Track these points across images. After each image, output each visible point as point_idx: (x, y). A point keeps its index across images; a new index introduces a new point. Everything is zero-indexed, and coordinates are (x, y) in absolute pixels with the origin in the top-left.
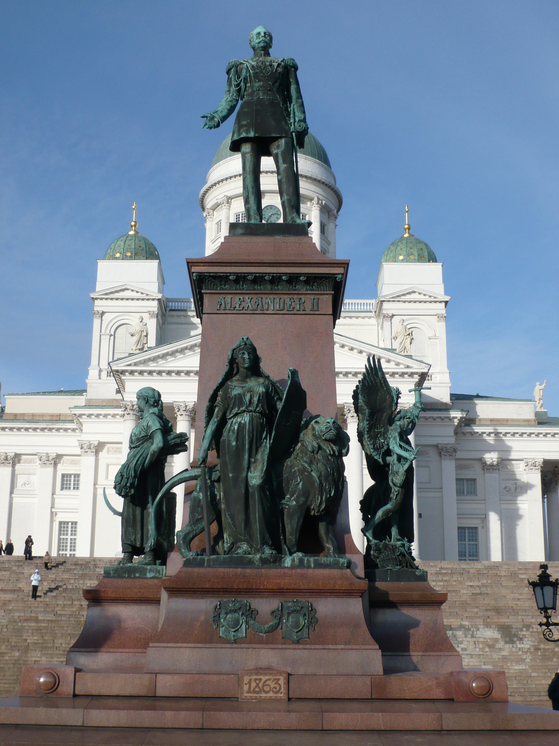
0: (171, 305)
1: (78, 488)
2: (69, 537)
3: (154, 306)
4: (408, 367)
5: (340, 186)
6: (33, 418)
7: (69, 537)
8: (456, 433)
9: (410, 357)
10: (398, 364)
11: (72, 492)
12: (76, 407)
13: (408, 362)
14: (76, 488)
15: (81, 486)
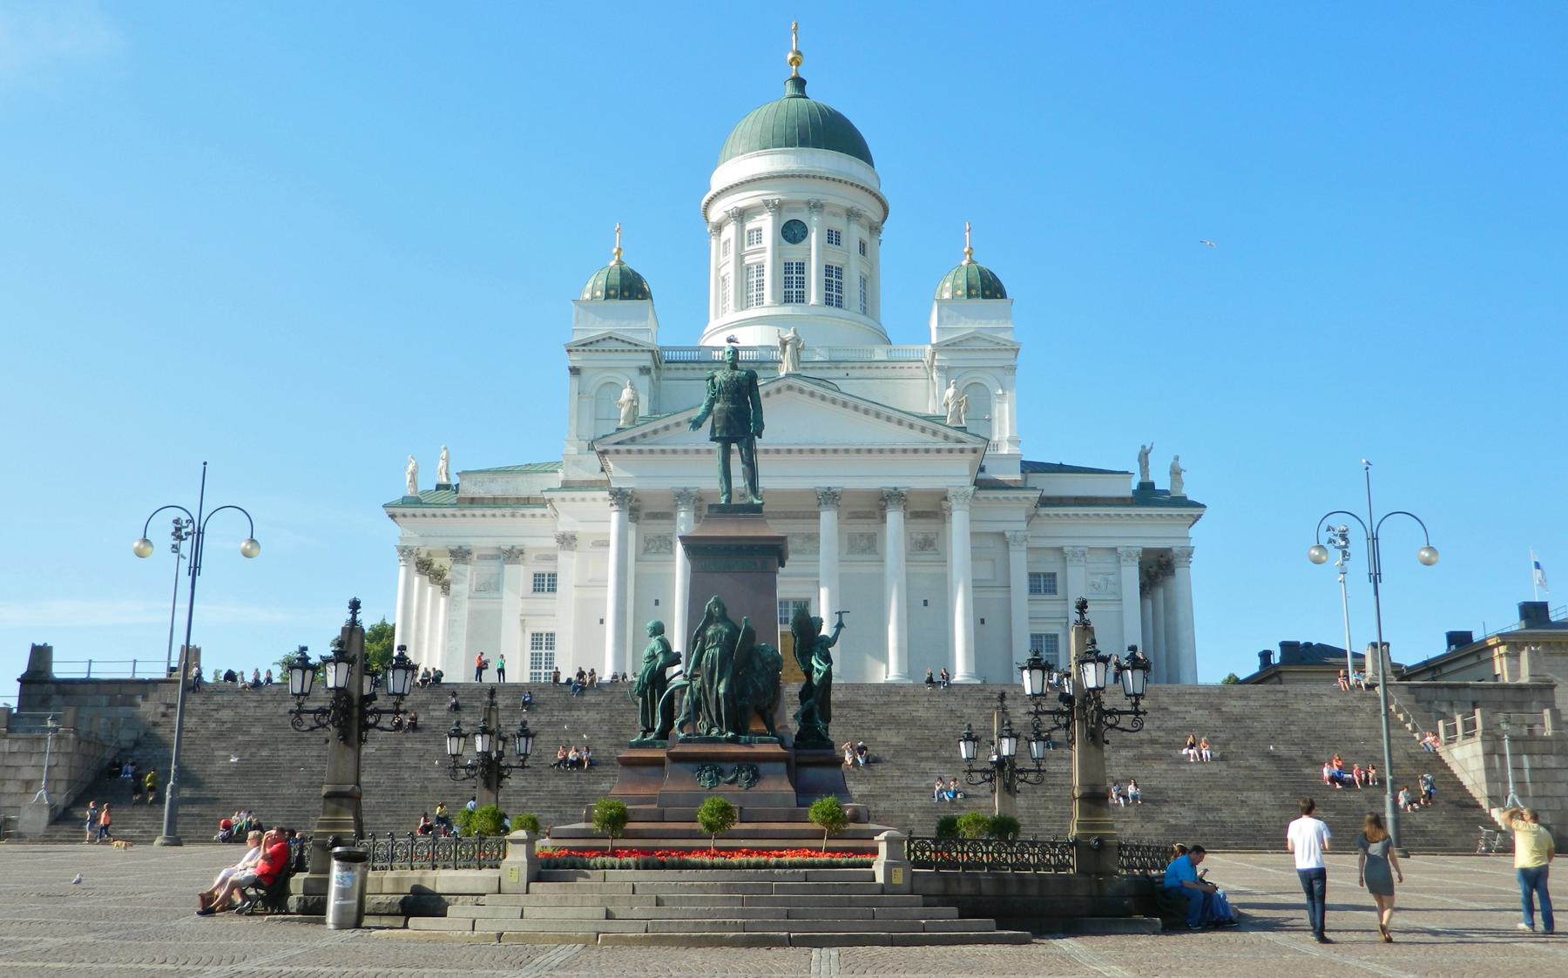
0: (668, 355)
1: (554, 590)
2: (544, 651)
3: (646, 359)
4: (960, 441)
5: (884, 192)
6: (495, 502)
7: (544, 651)
8: (1030, 519)
9: (964, 429)
10: (946, 437)
11: (546, 595)
12: (550, 490)
13: (961, 435)
14: (552, 589)
15: (559, 588)
